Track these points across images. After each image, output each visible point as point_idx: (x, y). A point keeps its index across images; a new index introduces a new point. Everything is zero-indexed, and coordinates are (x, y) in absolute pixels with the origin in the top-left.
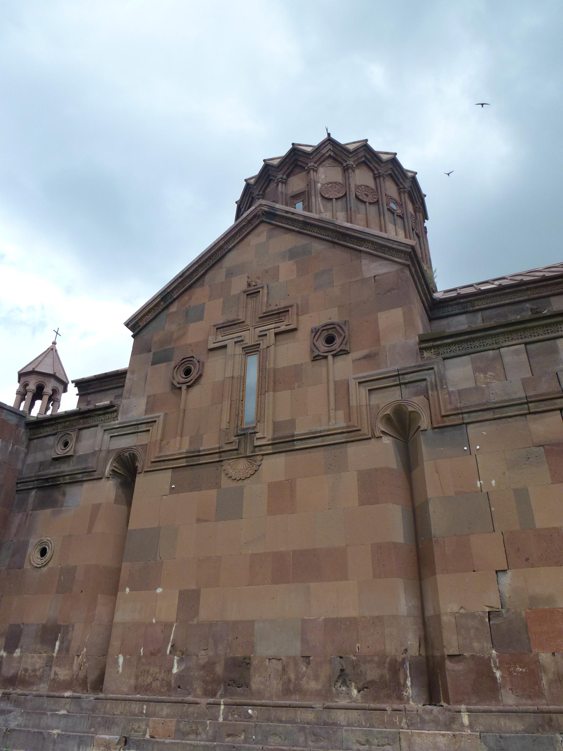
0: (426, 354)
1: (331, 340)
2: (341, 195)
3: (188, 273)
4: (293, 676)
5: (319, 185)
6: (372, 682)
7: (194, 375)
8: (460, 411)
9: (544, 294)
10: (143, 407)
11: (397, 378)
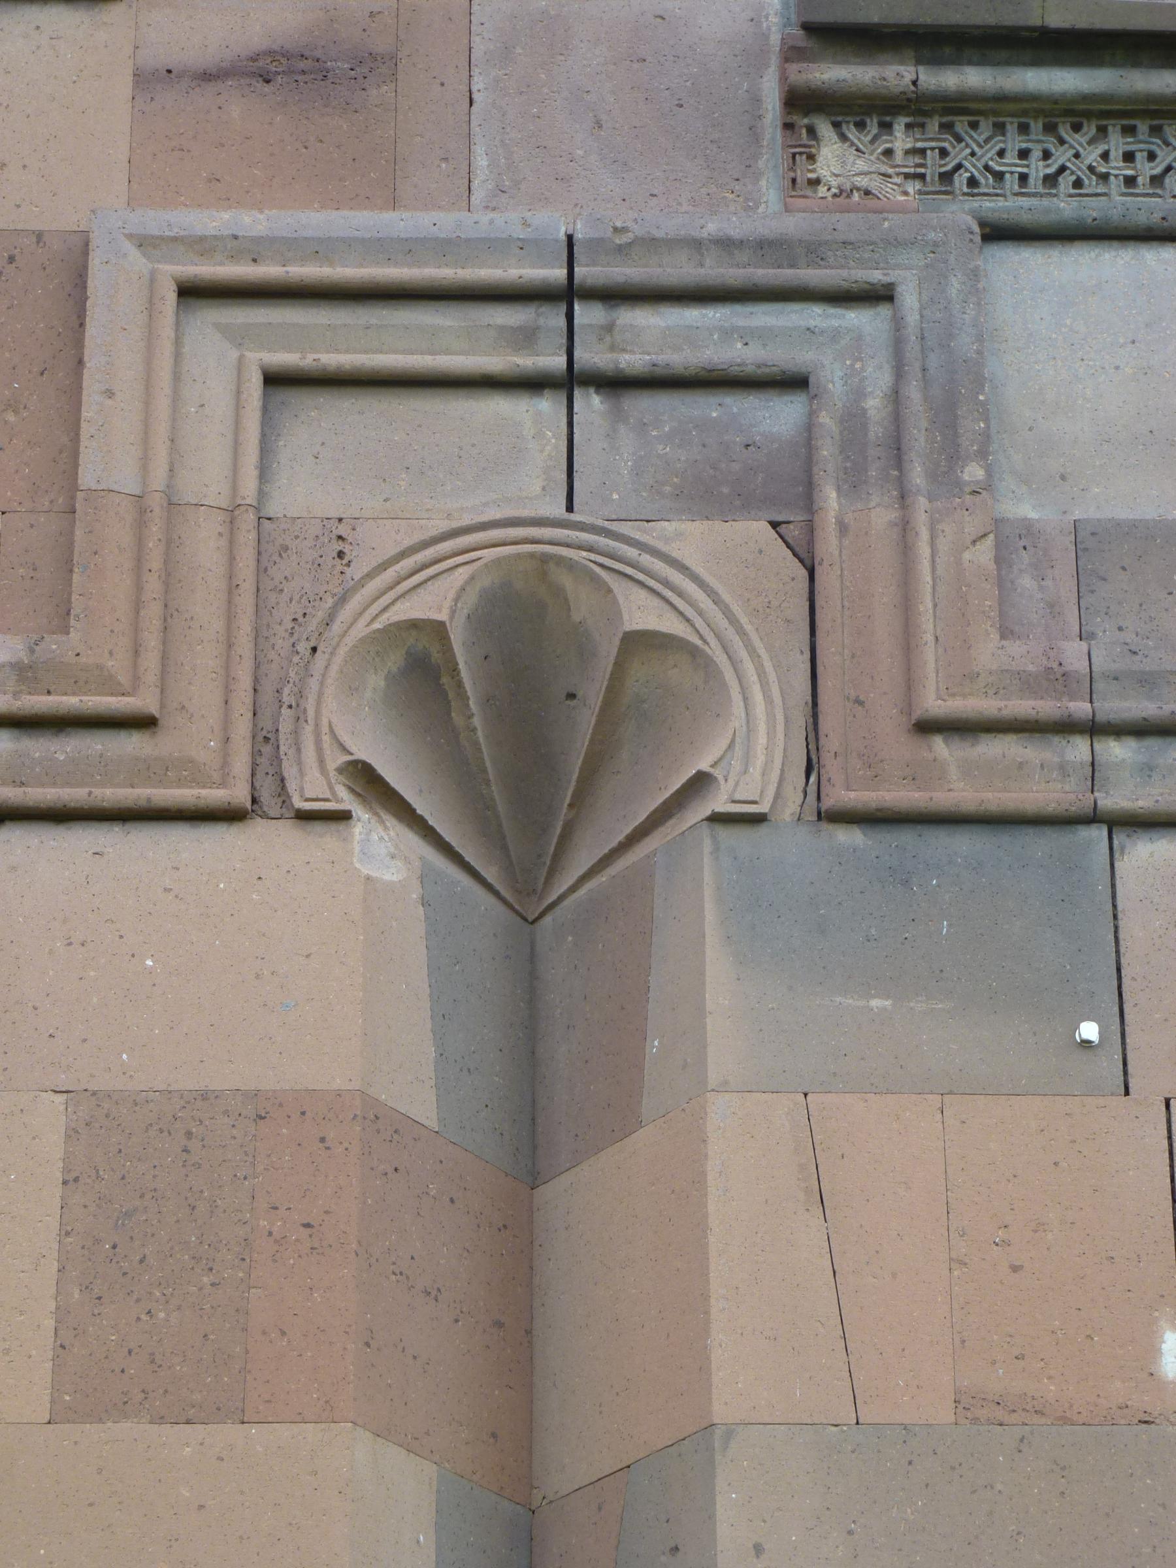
0: (837, 158)
8: (1080, 708)
11: (553, 318)
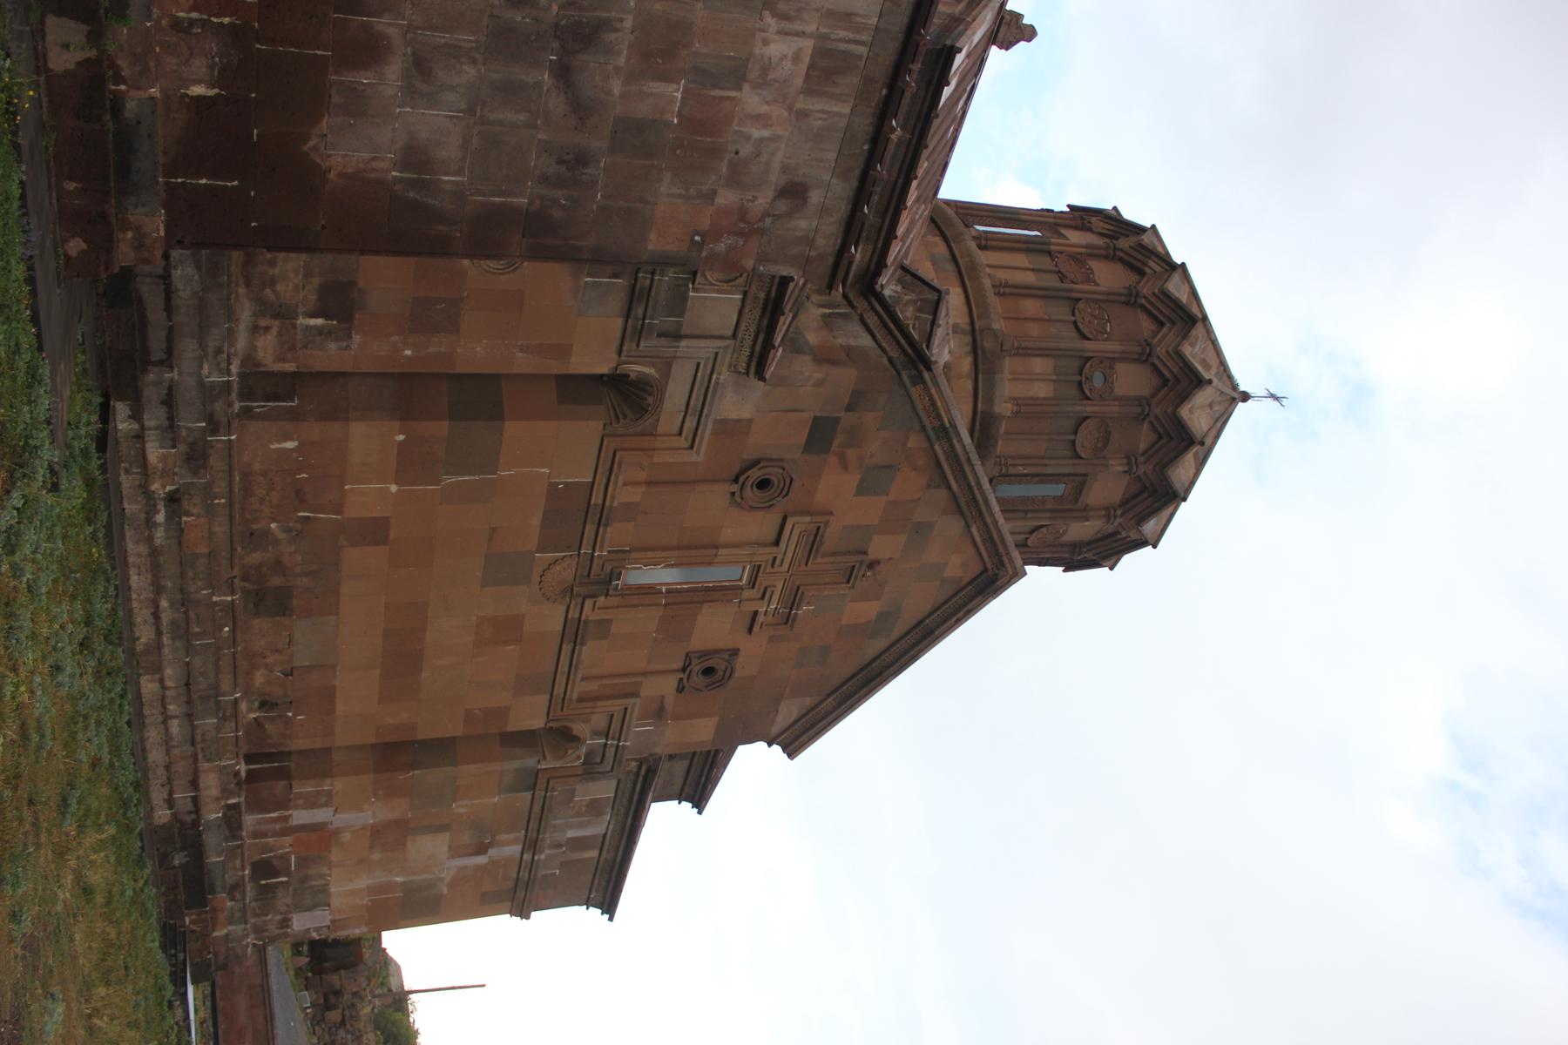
0: (634, 764)
4: (269, 660)
7: (751, 494)
10: (734, 415)
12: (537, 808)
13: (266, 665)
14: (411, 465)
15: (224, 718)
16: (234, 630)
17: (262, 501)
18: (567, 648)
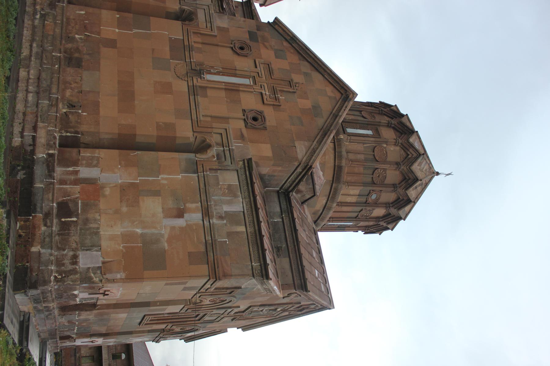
0: (241, 163)
1: (255, 120)
2: (377, 158)
3: (309, 52)
4: (73, 86)
5: (385, 146)
6: (69, 118)
9: (291, 255)
10: (222, 25)
12: (202, 186)
13: (71, 87)
14: (121, 24)
15: (52, 105)
16: (59, 67)
17: (73, 27)
18: (192, 98)
